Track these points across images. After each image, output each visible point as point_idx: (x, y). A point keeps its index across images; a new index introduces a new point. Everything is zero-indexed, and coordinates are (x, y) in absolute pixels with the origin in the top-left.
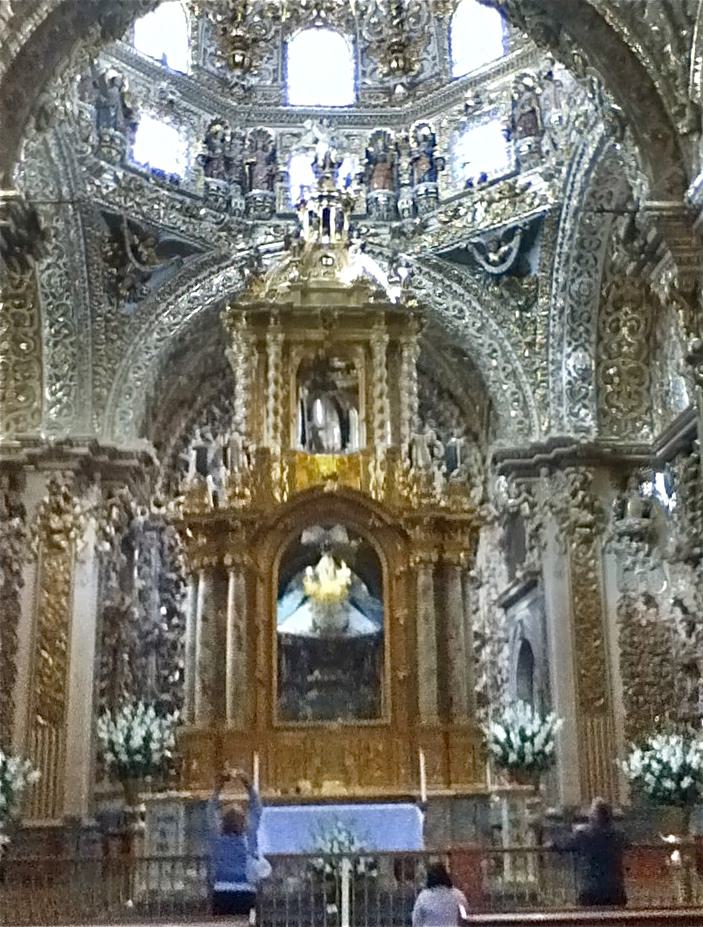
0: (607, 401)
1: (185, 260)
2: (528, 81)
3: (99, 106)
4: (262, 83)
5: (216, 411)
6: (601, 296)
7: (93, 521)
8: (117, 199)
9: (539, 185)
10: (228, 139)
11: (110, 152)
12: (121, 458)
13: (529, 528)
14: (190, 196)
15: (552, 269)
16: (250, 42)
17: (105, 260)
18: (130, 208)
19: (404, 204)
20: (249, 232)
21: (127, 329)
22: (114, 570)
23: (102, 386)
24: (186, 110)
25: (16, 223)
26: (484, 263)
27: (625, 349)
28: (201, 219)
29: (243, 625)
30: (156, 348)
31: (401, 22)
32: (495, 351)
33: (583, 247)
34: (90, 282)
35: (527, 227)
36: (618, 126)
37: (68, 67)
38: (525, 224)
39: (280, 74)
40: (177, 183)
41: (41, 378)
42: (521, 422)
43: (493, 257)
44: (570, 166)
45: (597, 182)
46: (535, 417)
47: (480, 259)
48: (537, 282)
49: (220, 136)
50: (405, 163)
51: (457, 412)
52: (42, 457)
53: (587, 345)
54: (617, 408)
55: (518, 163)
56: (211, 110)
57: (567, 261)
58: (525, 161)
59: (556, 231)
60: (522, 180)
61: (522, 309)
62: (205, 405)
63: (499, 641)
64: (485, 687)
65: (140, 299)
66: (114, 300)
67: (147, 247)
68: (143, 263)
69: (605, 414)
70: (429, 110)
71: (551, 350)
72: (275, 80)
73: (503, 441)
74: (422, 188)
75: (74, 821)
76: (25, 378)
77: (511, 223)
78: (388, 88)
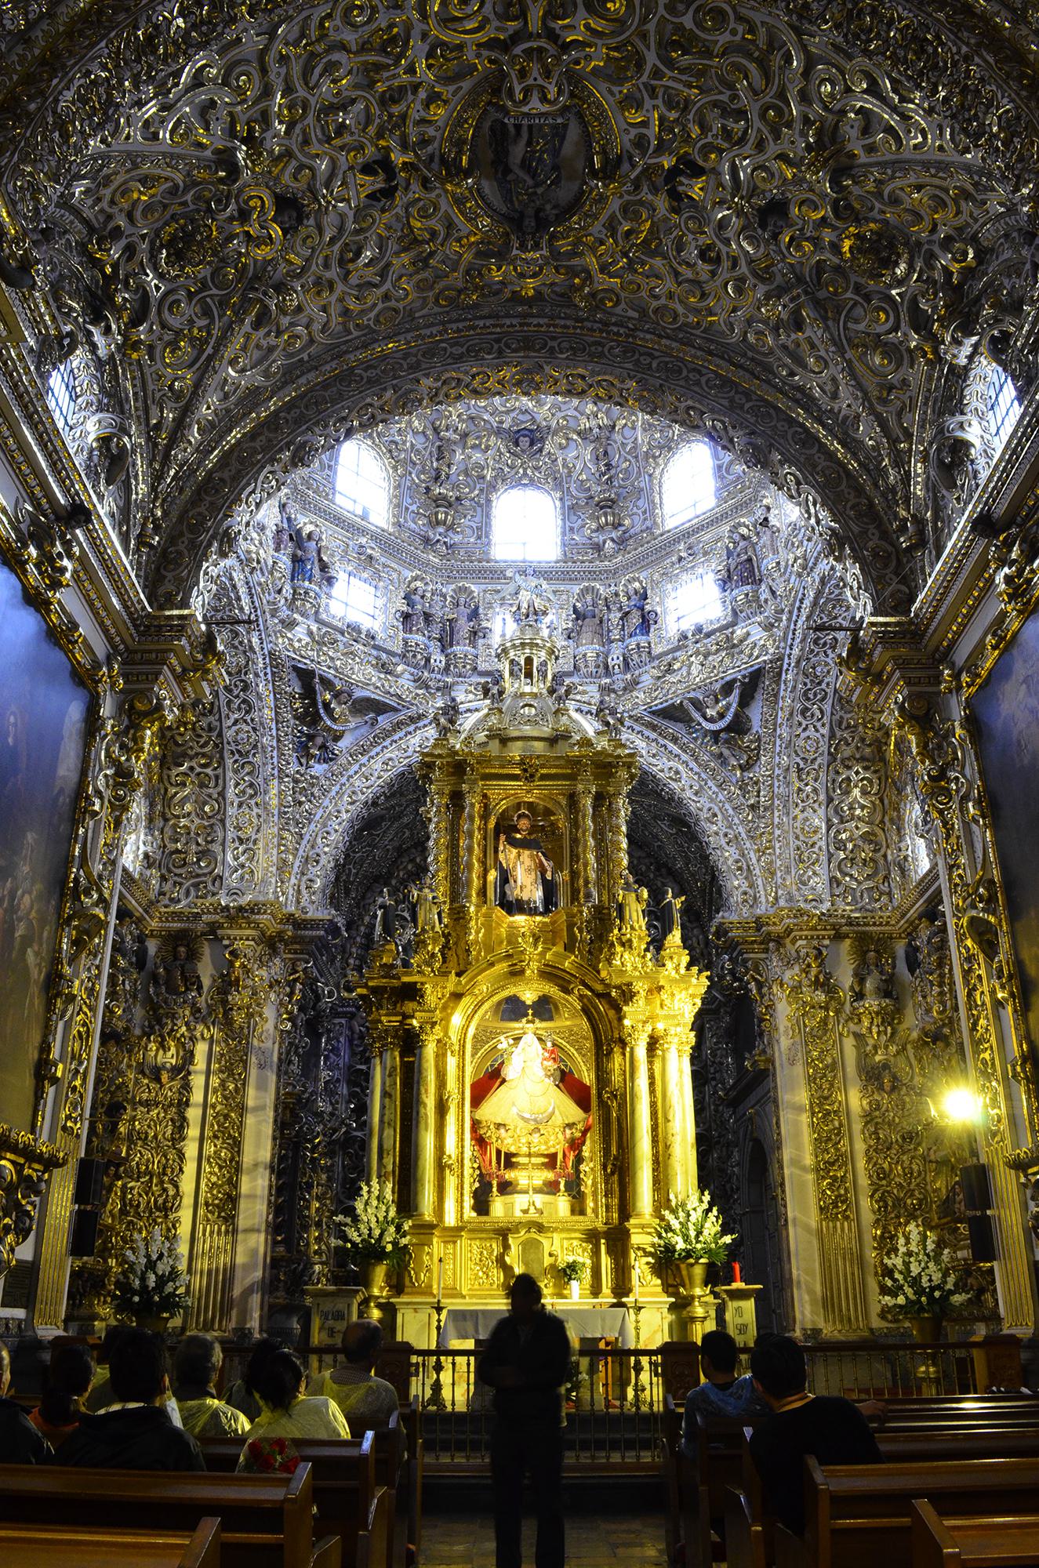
0: (841, 871)
2: (744, 531)
3: (296, 560)
6: (830, 753)
7: (273, 996)
9: (758, 634)
10: (428, 595)
12: (306, 929)
14: (385, 651)
15: (775, 724)
17: (296, 717)
18: (323, 663)
21: (315, 790)
22: (296, 1053)
23: (287, 851)
24: (385, 566)
25: (191, 645)
26: (701, 720)
27: (858, 812)
28: (398, 676)
30: (347, 811)
31: (610, 479)
32: (715, 815)
33: (808, 699)
34: (279, 741)
36: (836, 544)
37: (253, 492)
38: (744, 677)
39: (483, 531)
40: (373, 638)
41: (223, 844)
42: (745, 893)
43: (709, 712)
44: (791, 612)
46: (761, 888)
47: (696, 716)
48: (759, 740)
49: (420, 592)
50: (615, 616)
53: (816, 806)
54: (851, 876)
55: (735, 613)
56: (411, 566)
57: (791, 714)
60: (739, 632)
61: (743, 768)
63: (728, 1144)
65: (331, 760)
66: (303, 761)
67: (340, 703)
68: (334, 720)
69: (839, 884)
70: (641, 563)
71: (776, 814)
72: (479, 538)
73: (726, 914)
74: (632, 643)
76: (208, 842)
77: (730, 675)
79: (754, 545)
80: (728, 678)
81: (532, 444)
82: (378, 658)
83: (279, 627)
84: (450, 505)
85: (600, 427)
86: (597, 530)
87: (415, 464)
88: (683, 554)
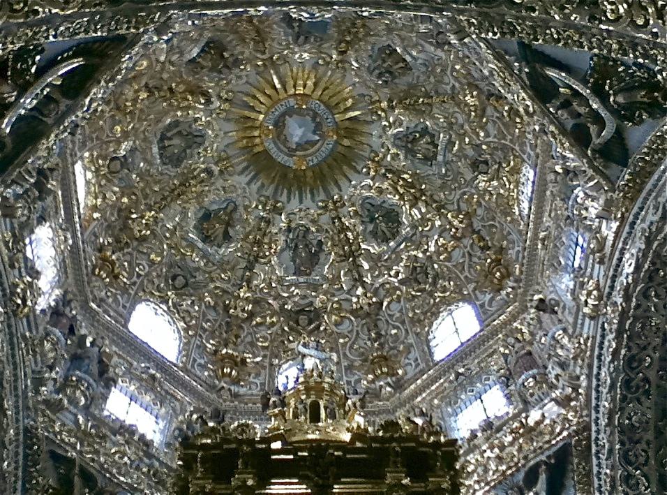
2: (519, 336)
4: (250, 392)
8: (73, 440)
9: (552, 409)
11: (74, 392)
14: (158, 460)
16: (239, 359)
35: (553, 461)
38: (549, 457)
45: (630, 361)
55: (525, 402)
57: (613, 487)
58: (532, 395)
59: (589, 461)
60: (534, 416)
78: (375, 389)
79: (531, 343)
80: (532, 463)
81: (310, 324)
82: (150, 466)
83: (43, 407)
84: (236, 365)
85: (369, 305)
86: (373, 381)
87: (205, 330)
88: (461, 370)
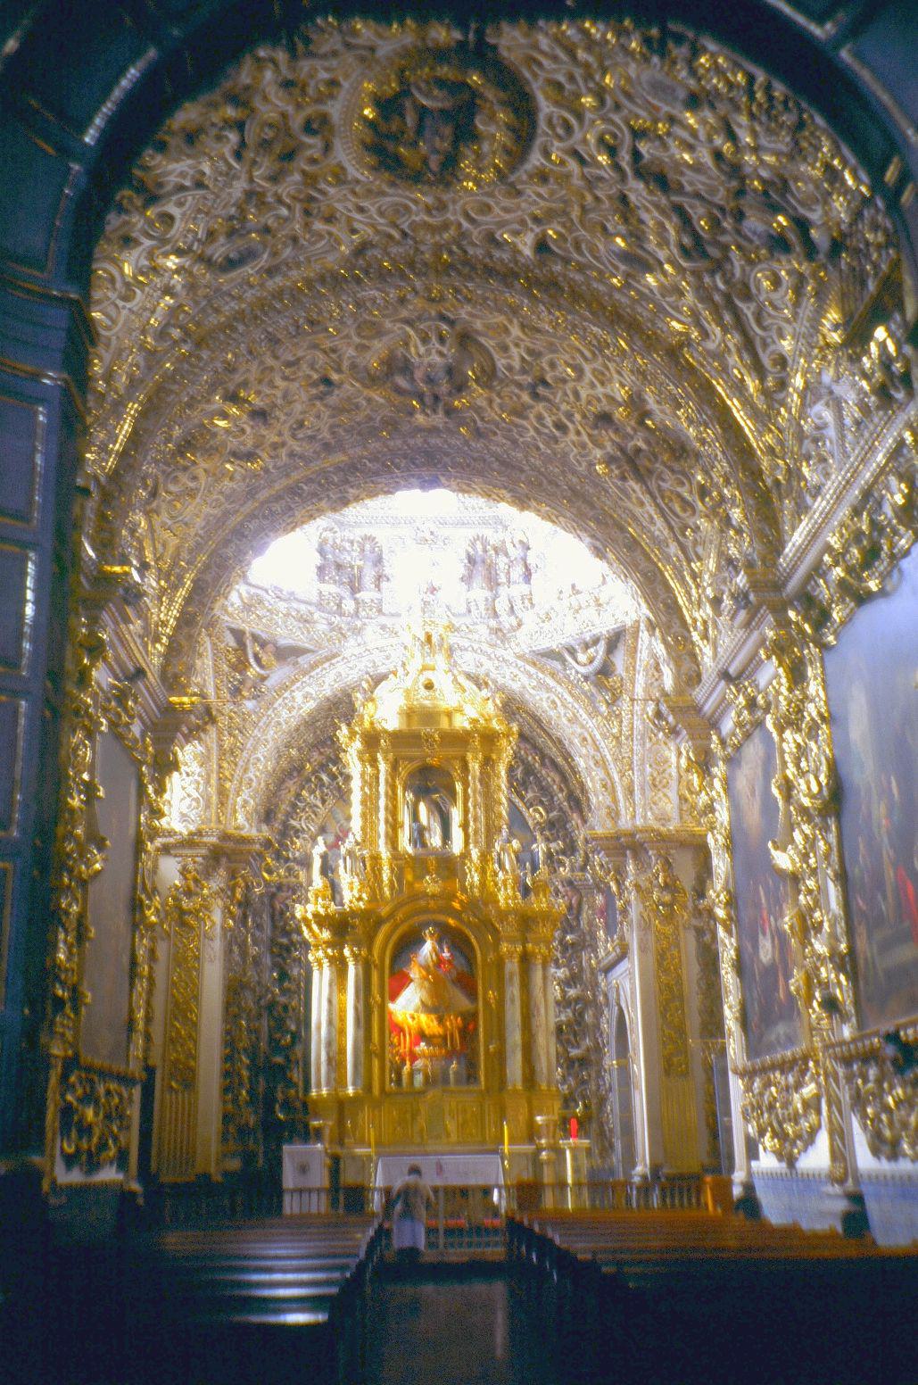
1: (299, 660)
5: (325, 778)
7: (220, 902)
13: (619, 904)
18: (250, 626)
19: (502, 606)
20: (358, 631)
22: (236, 943)
29: (361, 1007)
49: (331, 542)
51: (557, 779)
52: (175, 846)
62: (314, 772)
64: (588, 1050)
69: (686, 800)
75: (206, 1176)
